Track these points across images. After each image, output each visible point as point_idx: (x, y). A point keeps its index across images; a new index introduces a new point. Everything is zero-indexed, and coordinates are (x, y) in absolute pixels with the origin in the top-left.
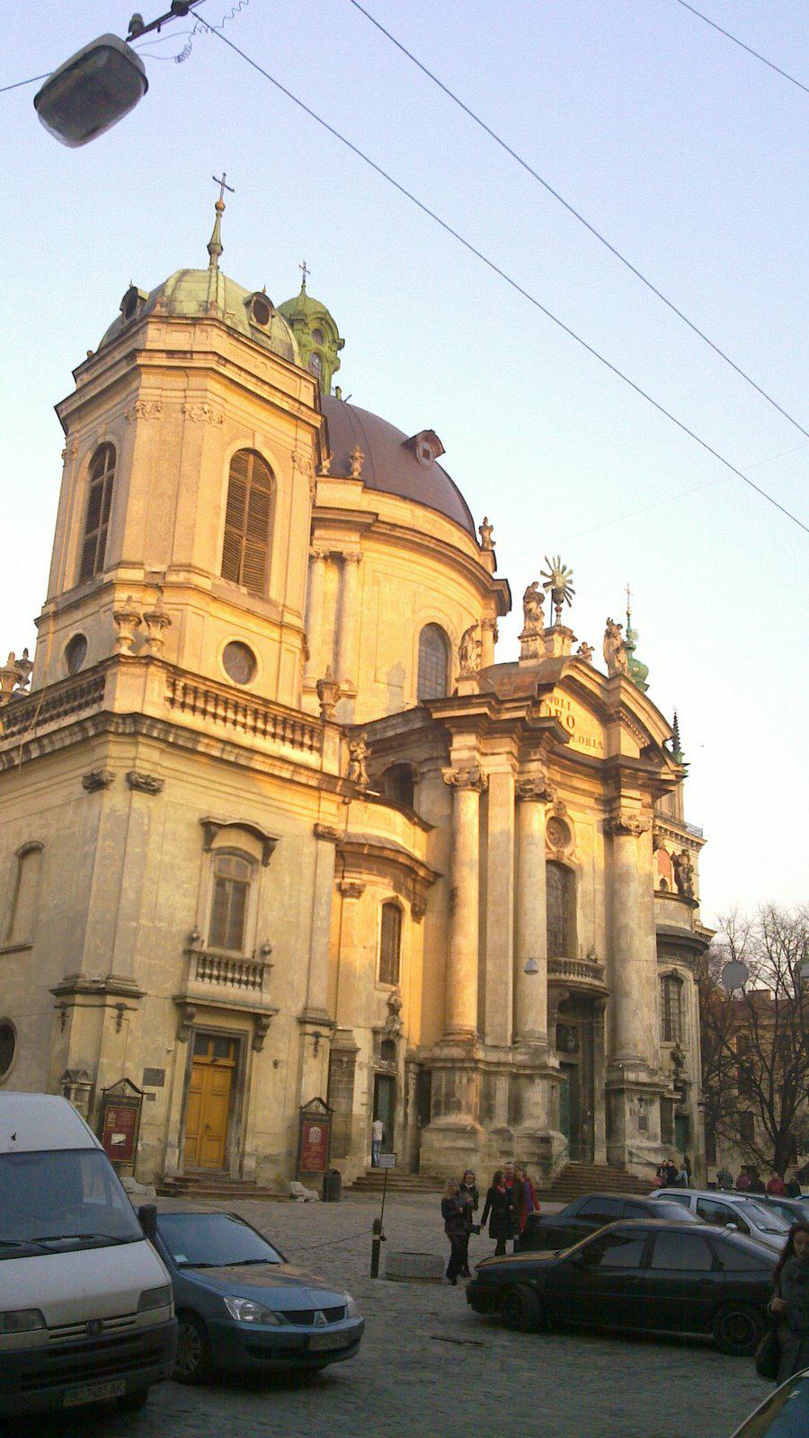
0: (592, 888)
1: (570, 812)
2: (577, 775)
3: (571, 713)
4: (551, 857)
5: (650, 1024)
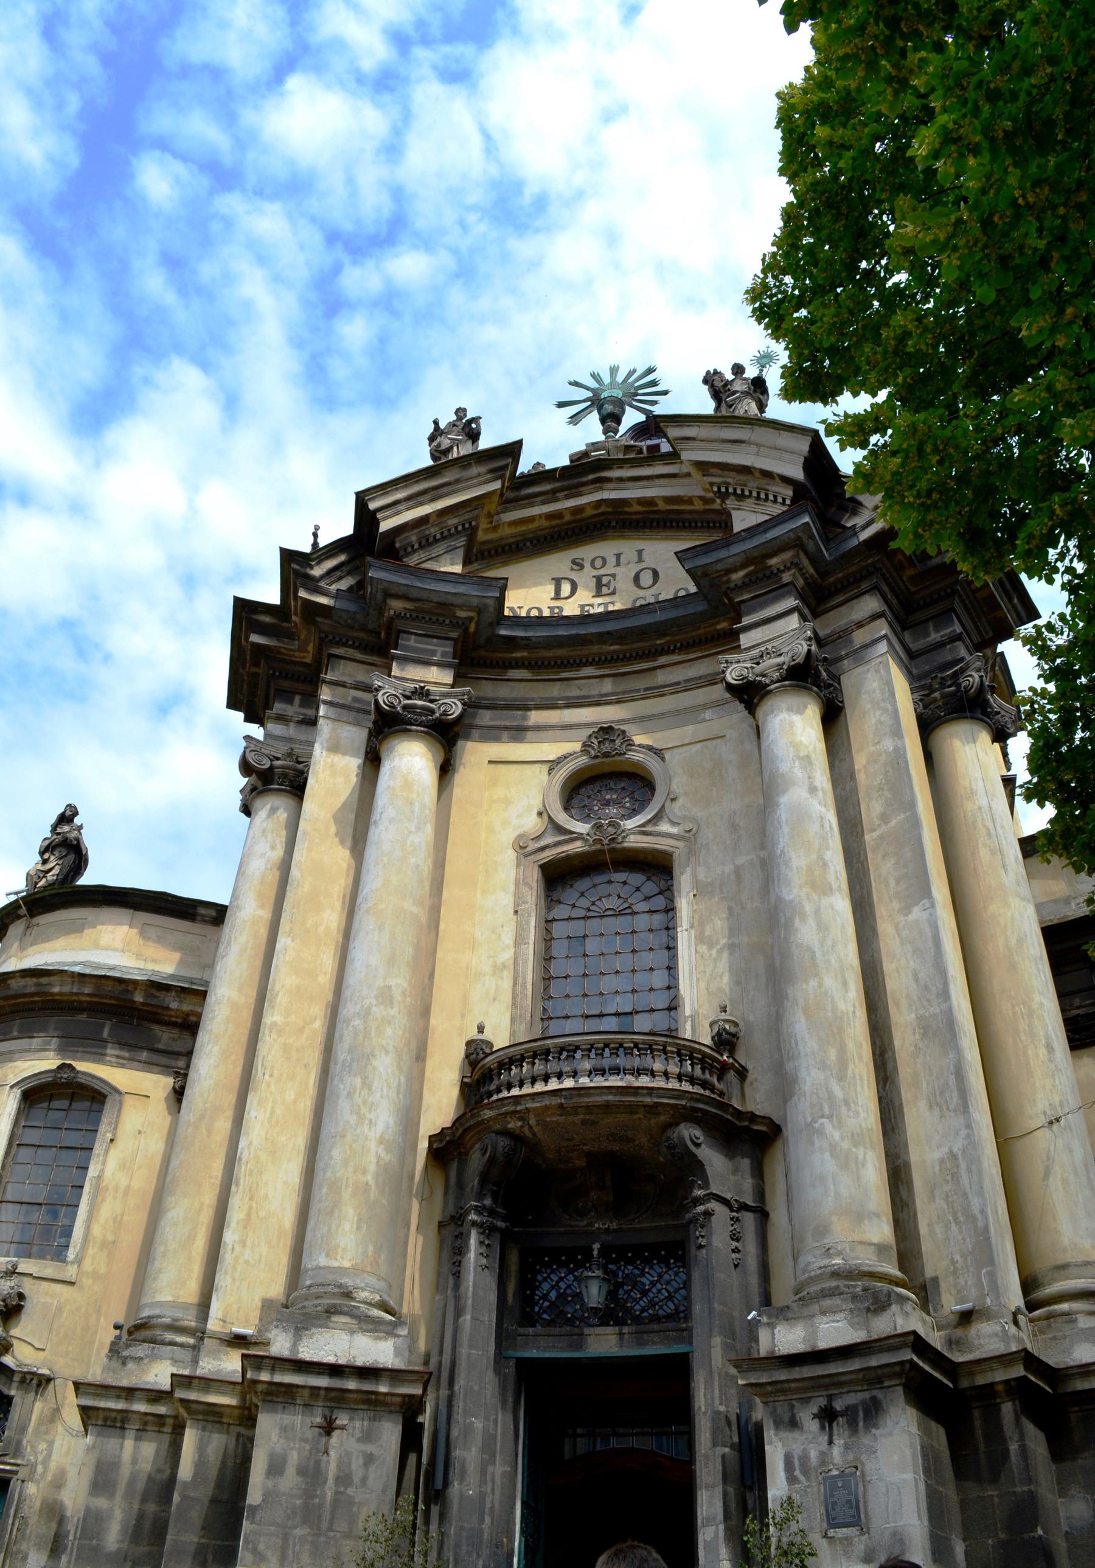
0: (728, 869)
1: (638, 739)
2: (663, 660)
3: (649, 561)
4: (577, 847)
5: (953, 1156)
